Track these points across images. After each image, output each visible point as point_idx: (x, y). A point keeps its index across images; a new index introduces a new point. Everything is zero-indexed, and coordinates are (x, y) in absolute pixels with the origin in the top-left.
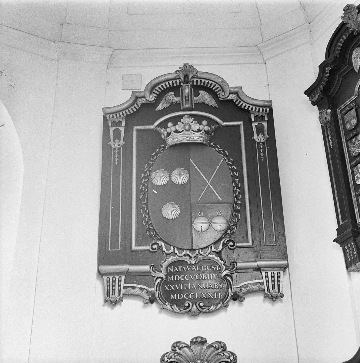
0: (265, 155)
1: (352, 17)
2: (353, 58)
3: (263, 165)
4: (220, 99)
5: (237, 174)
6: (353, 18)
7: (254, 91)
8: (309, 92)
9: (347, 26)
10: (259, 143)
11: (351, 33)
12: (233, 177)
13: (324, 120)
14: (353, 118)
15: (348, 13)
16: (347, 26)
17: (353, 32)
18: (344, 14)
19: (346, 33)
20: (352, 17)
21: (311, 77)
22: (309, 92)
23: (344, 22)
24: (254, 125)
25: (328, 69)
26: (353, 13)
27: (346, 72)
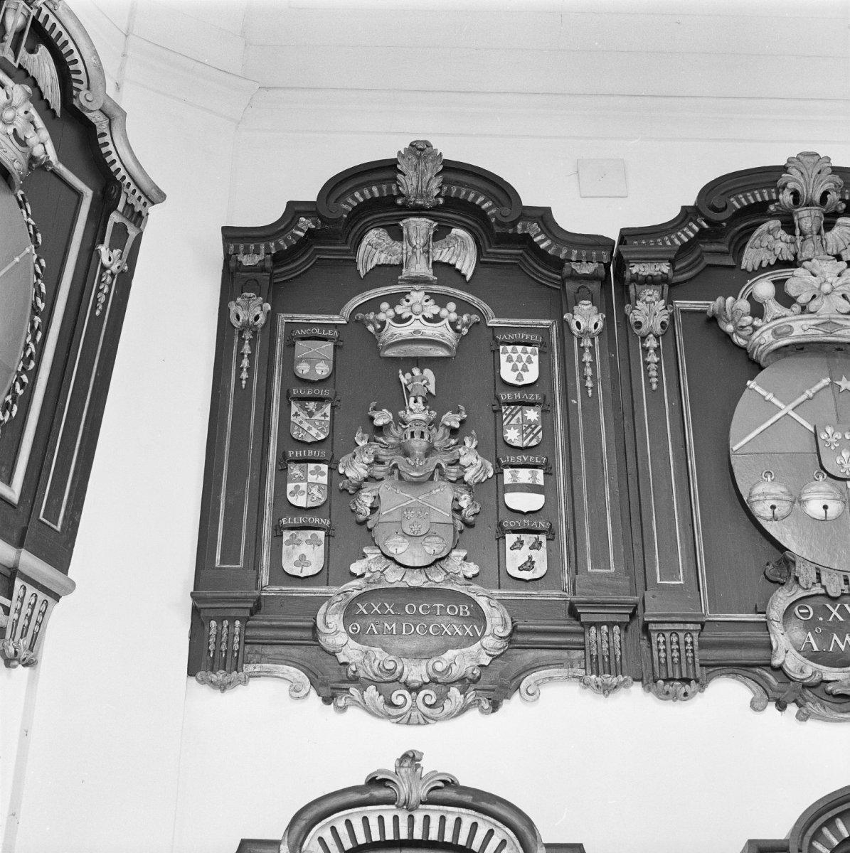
0: (105, 305)
1: (423, 172)
2: (365, 242)
3: (96, 322)
4: (76, 103)
5: (42, 306)
6: (423, 173)
7: (141, 146)
8: (232, 236)
9: (399, 176)
10: (104, 268)
11: (395, 194)
12: (35, 310)
13: (251, 319)
14: (326, 360)
15: (419, 158)
16: (399, 176)
17: (401, 195)
18: (405, 149)
19: (384, 187)
20: (423, 172)
21: (264, 211)
22: (232, 236)
23: (399, 167)
24: (115, 218)
25: (305, 223)
26: (430, 165)
27: (333, 255)
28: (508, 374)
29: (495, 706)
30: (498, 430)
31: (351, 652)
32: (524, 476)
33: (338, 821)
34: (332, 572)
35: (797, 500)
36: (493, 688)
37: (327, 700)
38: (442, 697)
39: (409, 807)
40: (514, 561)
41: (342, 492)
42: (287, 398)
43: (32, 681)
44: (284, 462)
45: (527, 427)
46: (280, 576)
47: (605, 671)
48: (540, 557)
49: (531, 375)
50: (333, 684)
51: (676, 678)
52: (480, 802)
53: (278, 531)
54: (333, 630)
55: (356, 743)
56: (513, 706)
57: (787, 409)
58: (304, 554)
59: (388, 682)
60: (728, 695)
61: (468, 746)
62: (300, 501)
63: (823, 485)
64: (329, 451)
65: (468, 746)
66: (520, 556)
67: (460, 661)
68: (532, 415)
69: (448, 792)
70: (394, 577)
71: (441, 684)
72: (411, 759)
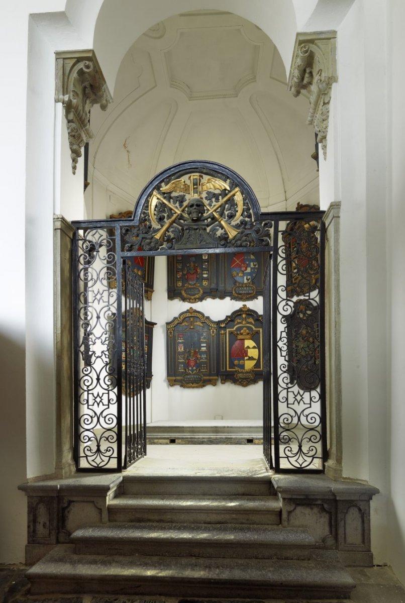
28: (204, 258)
29: (202, 301)
30: (202, 266)
31: (185, 295)
32: (205, 272)
33: (184, 315)
34: (183, 286)
35: (238, 274)
36: (201, 299)
37: (183, 301)
38: (196, 300)
39: (191, 313)
40: (204, 283)
41: (183, 275)
42: (176, 263)
43: (151, 302)
44: (177, 272)
45: (205, 265)
46: (177, 286)
47: (214, 297)
48: (207, 283)
49: (206, 258)
50: (184, 300)
51: (222, 298)
52: (199, 312)
53: (176, 281)
54: (183, 292)
55: (186, 306)
56: (204, 301)
57: (238, 262)
58: (180, 284)
59: (190, 299)
60: (228, 299)
61: (198, 306)
62: (179, 277)
63: (241, 272)
64: (182, 270)
65: (198, 306)
66: (205, 283)
67: (197, 296)
68: (206, 264)
69: (196, 311)
70: (190, 287)
71: (195, 299)
72: (191, 308)
